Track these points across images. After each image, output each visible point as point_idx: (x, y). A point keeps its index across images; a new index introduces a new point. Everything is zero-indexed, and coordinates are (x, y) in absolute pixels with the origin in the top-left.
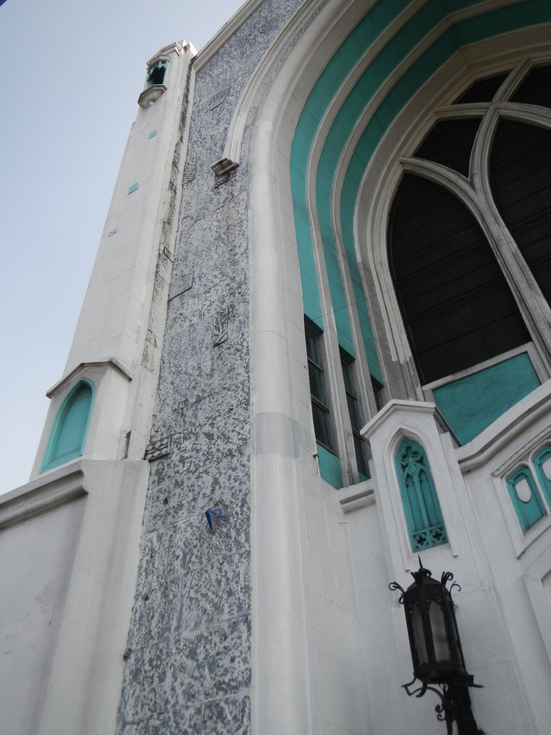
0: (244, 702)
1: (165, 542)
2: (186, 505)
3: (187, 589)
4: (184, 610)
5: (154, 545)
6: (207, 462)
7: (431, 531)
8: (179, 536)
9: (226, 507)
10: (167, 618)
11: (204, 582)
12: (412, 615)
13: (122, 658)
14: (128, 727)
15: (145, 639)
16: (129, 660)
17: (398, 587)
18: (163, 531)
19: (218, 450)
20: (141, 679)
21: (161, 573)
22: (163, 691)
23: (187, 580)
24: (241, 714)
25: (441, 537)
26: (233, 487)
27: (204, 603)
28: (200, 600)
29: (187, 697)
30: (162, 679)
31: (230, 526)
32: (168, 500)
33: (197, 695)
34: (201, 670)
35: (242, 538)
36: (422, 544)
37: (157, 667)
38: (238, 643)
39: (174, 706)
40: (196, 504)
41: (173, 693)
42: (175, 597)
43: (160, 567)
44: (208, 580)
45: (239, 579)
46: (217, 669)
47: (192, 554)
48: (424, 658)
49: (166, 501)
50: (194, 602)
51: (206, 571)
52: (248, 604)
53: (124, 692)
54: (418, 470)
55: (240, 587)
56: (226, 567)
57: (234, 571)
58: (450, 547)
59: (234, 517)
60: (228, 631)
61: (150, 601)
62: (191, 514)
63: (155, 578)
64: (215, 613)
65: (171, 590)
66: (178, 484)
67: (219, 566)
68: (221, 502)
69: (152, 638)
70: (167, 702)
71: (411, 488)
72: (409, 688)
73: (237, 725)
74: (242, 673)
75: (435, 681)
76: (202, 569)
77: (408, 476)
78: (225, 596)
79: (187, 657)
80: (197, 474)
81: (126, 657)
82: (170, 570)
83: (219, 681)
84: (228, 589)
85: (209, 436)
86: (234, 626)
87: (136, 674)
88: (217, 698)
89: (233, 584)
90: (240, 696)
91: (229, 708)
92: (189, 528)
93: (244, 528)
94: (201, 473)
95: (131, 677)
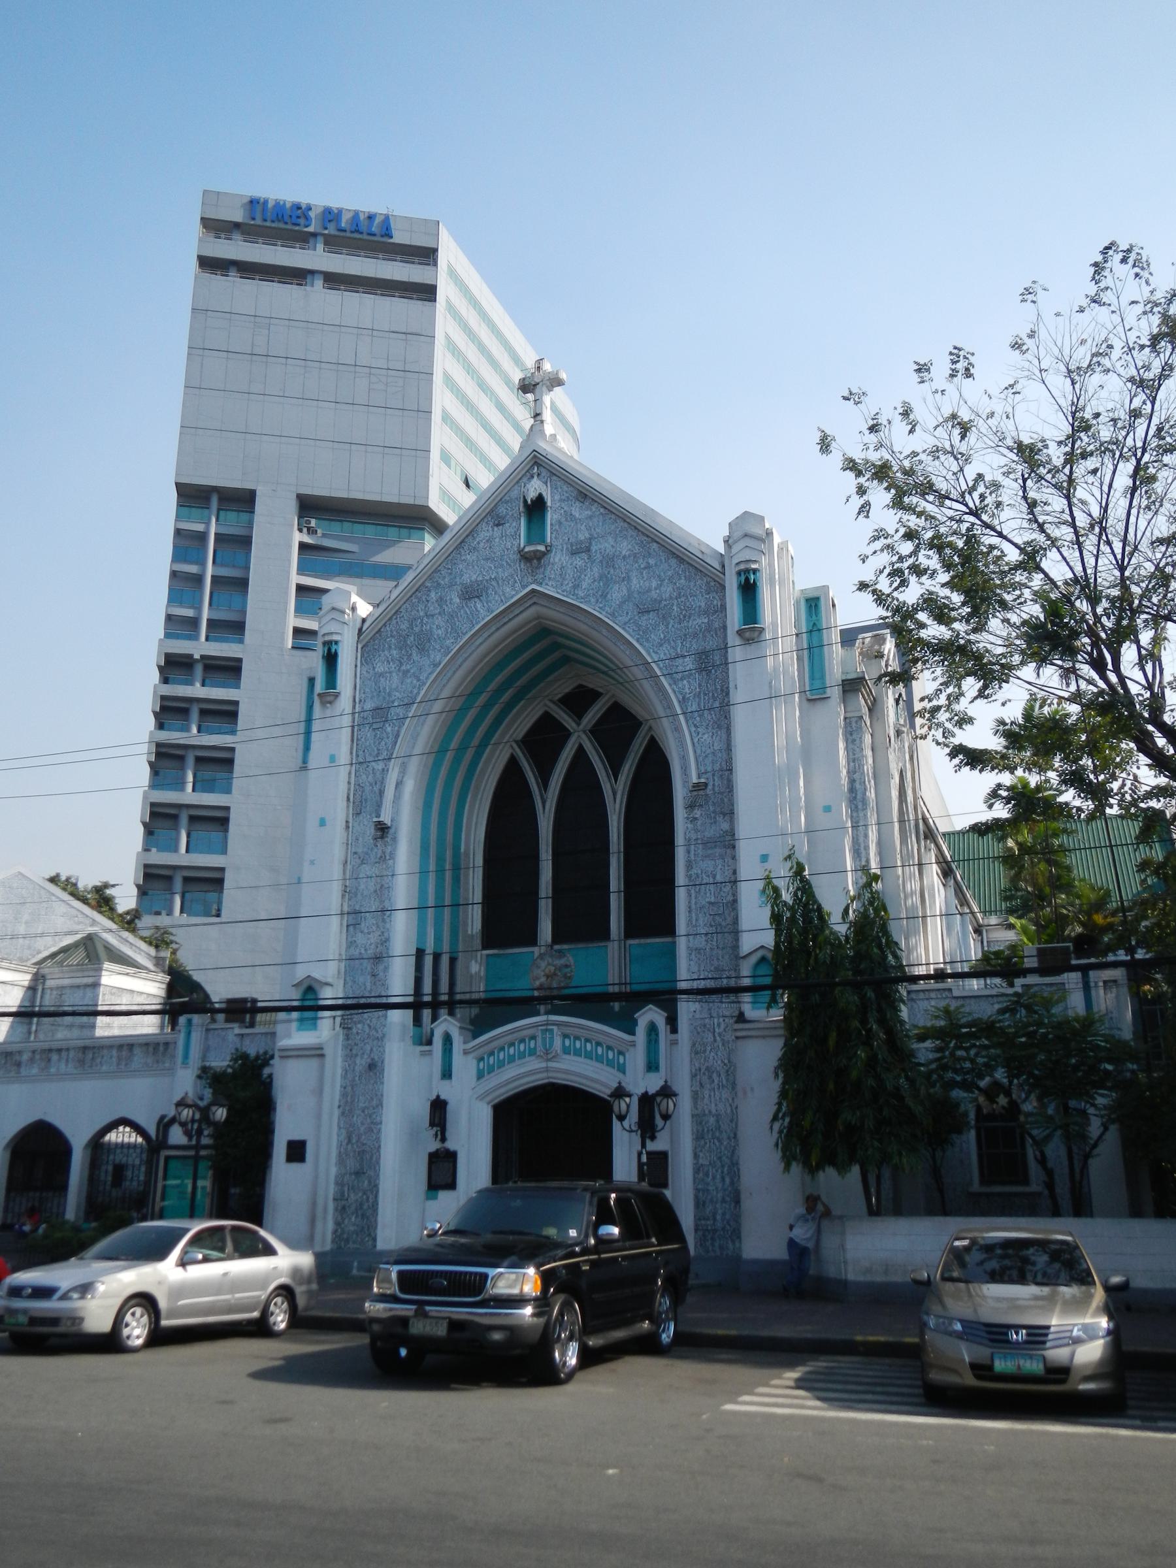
66: (356, 1044)
81: (339, 1107)
85: (369, 1026)
86: (377, 1106)
87: (343, 1113)
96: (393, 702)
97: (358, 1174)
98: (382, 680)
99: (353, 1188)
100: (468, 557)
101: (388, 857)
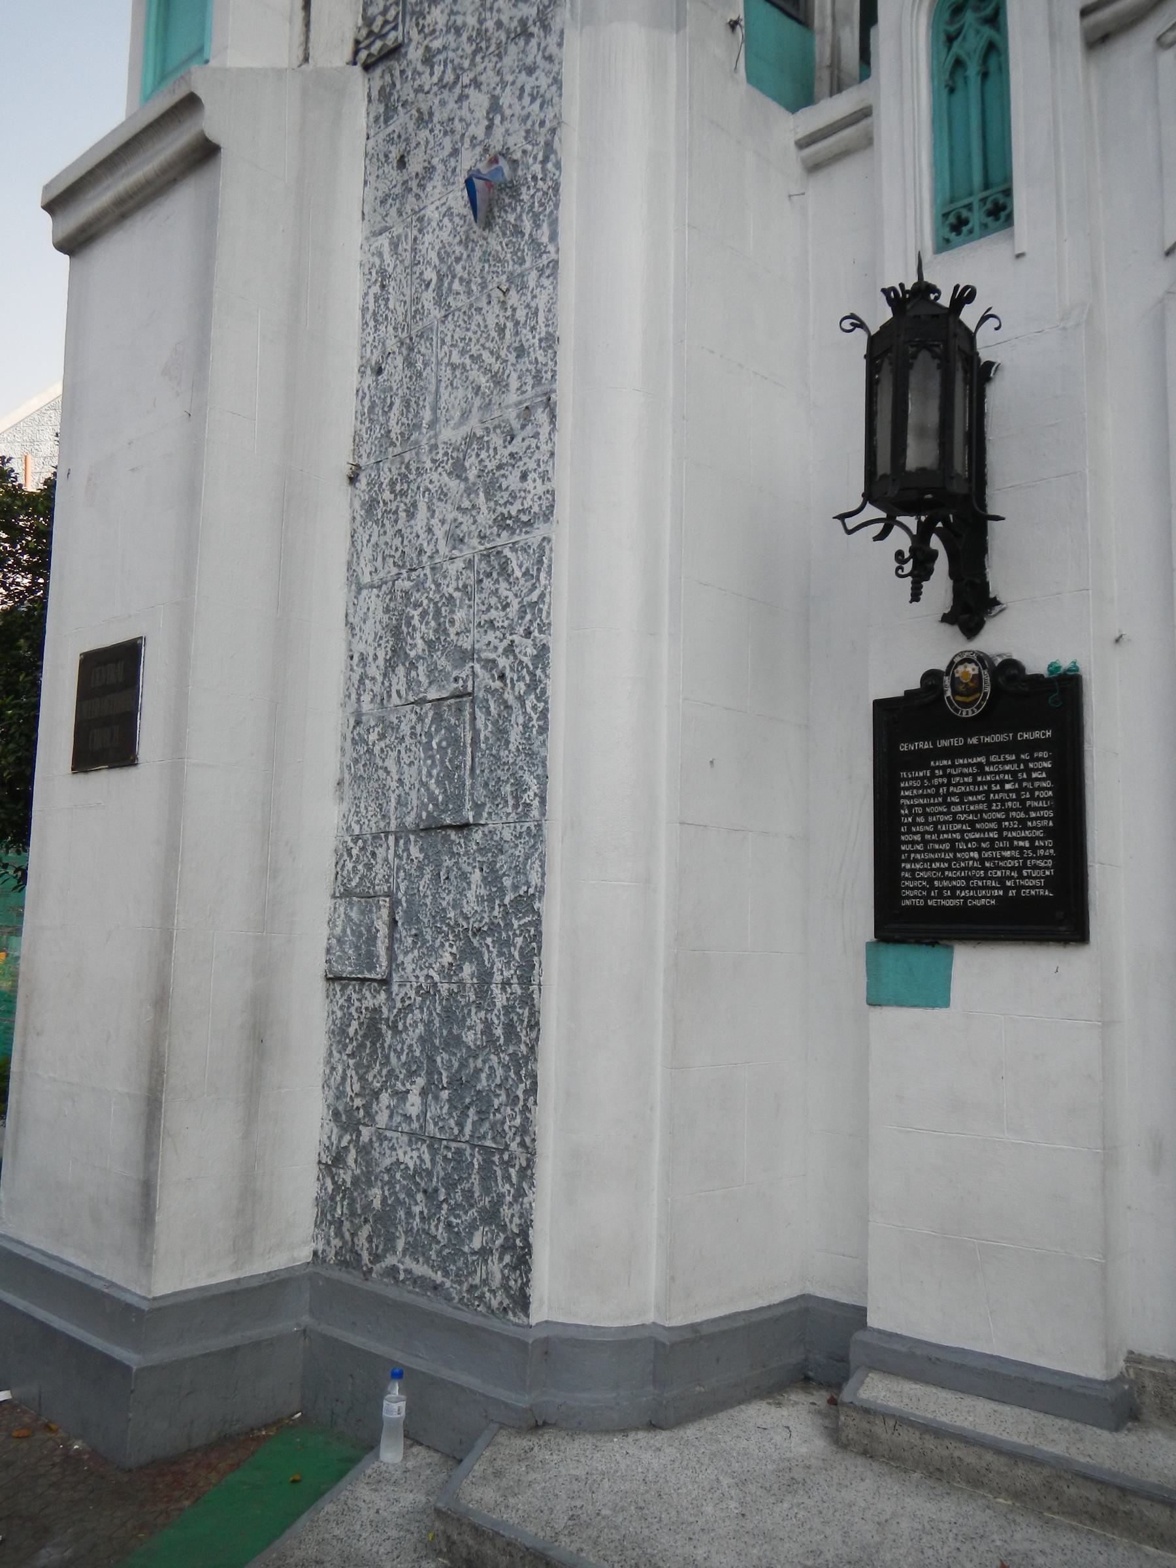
0: (541, 548)
1: (404, 254)
2: (440, 167)
3: (446, 348)
4: (442, 390)
5: (386, 263)
6: (478, 59)
7: (984, 201)
8: (428, 238)
9: (514, 163)
10: (415, 406)
11: (475, 333)
12: (878, 381)
13: (346, 481)
14: (365, 592)
15: (381, 446)
16: (357, 484)
17: (859, 324)
18: (400, 230)
19: (499, 25)
20: (379, 517)
21: (400, 319)
22: (414, 535)
23: (445, 331)
24: (535, 568)
25: (1003, 215)
26: (529, 115)
27: (475, 374)
28: (468, 368)
29: (451, 542)
30: (411, 515)
31: (522, 207)
32: (406, 159)
33: (466, 540)
34: (472, 496)
35: (544, 236)
36: (959, 233)
37: (403, 494)
38: (534, 445)
39: (431, 557)
40: (458, 164)
41: (429, 537)
42: (426, 364)
43: (398, 308)
44: (482, 329)
45: (537, 322)
46: (499, 494)
47: (454, 277)
48: (884, 465)
49: (402, 163)
50: (458, 373)
51: (479, 310)
52: (552, 370)
53: (356, 538)
54: (983, 43)
55: (537, 337)
56: (513, 298)
57: (528, 306)
58: (1012, 236)
59: (529, 188)
60: (516, 425)
61: (385, 375)
62: (450, 188)
63: (390, 329)
64: (495, 392)
65: (419, 352)
67: (502, 299)
68: (505, 153)
69: (393, 444)
70: (421, 552)
71: (959, 95)
72: (847, 520)
73: (529, 584)
74: (540, 498)
75: (908, 512)
76: (471, 306)
77: (959, 64)
78: (512, 358)
79: (450, 474)
80: (457, 90)
81: (353, 479)
82: (416, 312)
83: (502, 514)
84: (517, 344)
87: (370, 506)
88: (498, 542)
89: (526, 333)
90: (534, 538)
91: (518, 558)
92: (446, 220)
93: (547, 212)
94: (466, 86)
95: (363, 513)
97: (430, 829)
99: (412, 918)
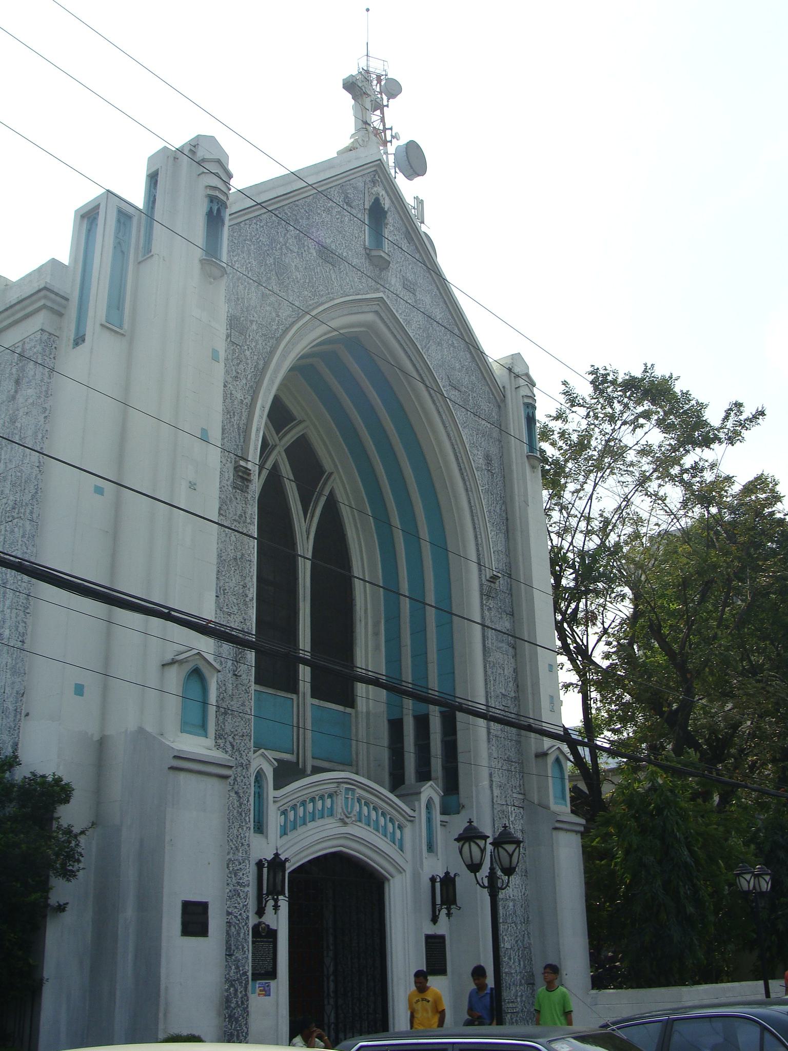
60: (242, 862)
78: (240, 844)
85: (233, 746)
96: (252, 322)
98: (241, 287)
100: (324, 215)
101: (248, 521)
